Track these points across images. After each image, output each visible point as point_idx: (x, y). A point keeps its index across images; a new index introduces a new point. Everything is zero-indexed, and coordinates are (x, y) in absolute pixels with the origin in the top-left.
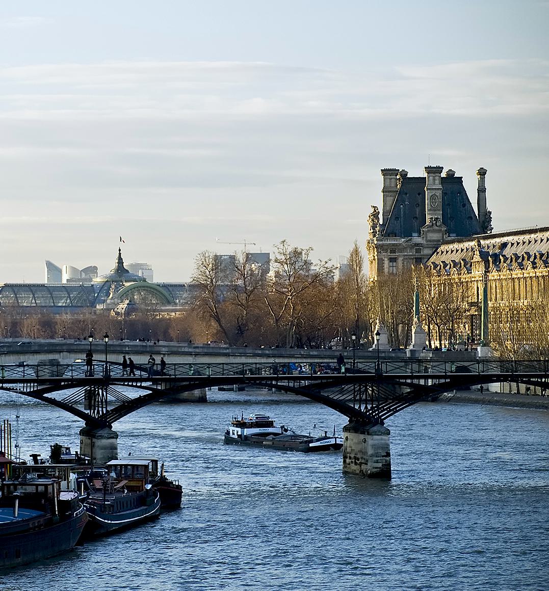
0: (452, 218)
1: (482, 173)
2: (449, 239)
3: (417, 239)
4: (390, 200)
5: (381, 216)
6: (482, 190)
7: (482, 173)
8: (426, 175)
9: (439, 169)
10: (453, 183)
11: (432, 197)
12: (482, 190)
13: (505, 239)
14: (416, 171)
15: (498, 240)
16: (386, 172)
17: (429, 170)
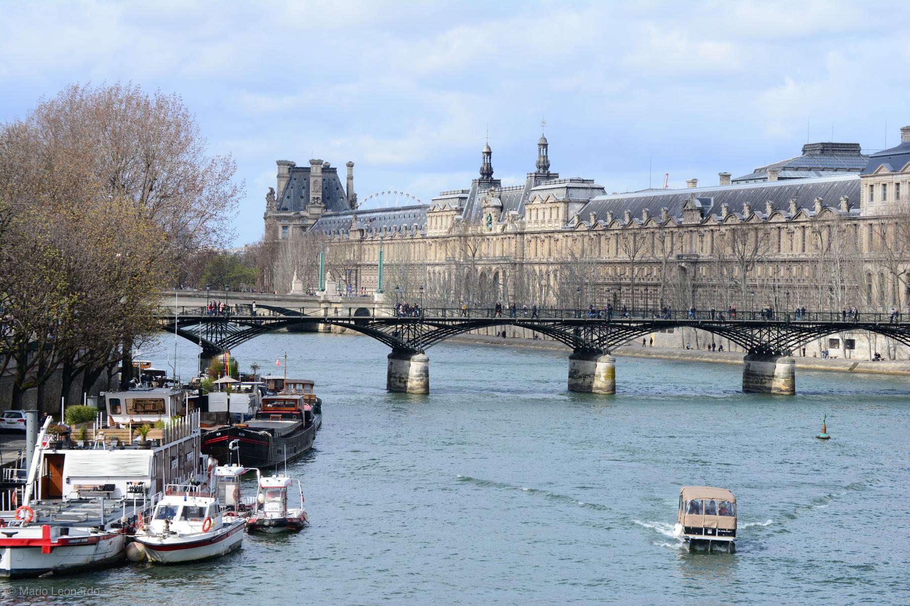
0: (329, 198)
1: (350, 165)
2: (327, 213)
3: (303, 213)
4: (283, 183)
5: (276, 195)
6: (350, 178)
7: (350, 165)
8: (309, 166)
9: (319, 162)
10: (328, 170)
11: (315, 182)
12: (350, 178)
13: (375, 214)
14: (302, 162)
15: (368, 215)
16: (280, 163)
17: (313, 162)
